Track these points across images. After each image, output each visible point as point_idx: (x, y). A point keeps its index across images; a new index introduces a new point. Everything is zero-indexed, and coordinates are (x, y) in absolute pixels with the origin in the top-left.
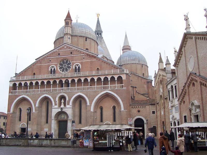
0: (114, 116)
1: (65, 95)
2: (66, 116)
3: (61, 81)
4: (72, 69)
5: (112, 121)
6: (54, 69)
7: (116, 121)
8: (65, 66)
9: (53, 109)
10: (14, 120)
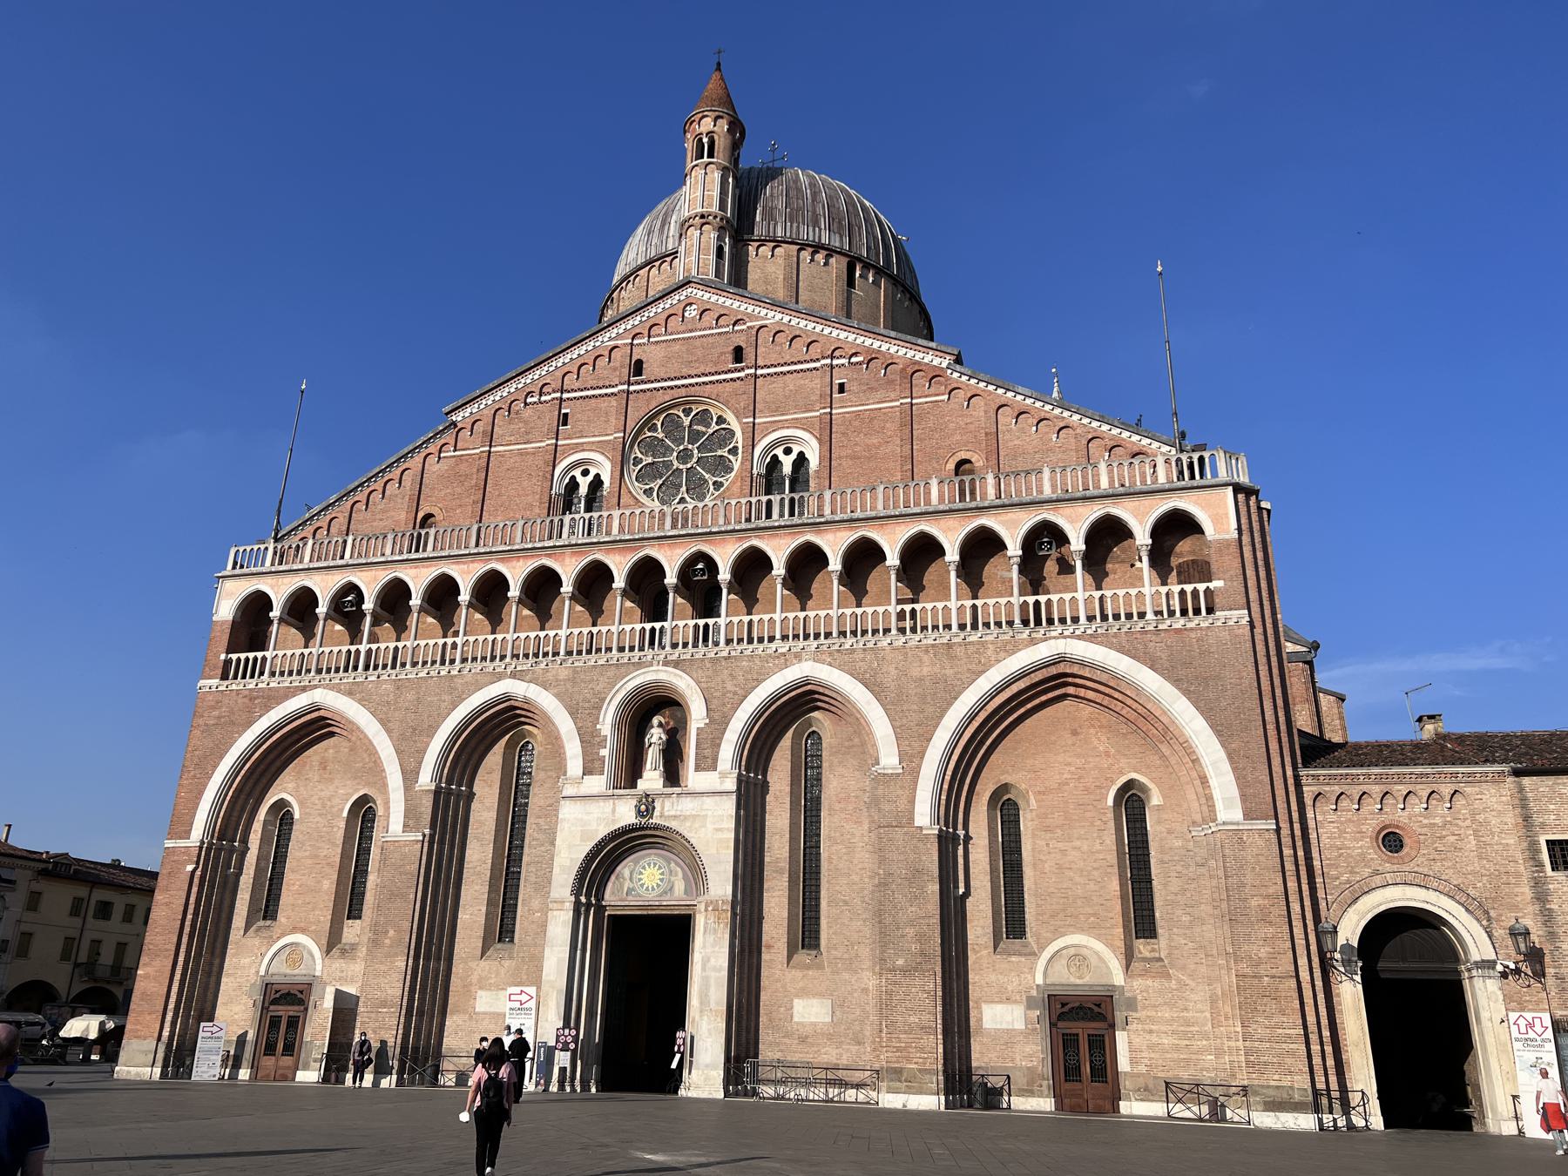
1: (684, 684)
3: (646, 575)
4: (740, 477)
7: (1160, 931)
8: (685, 456)
9: (567, 811)
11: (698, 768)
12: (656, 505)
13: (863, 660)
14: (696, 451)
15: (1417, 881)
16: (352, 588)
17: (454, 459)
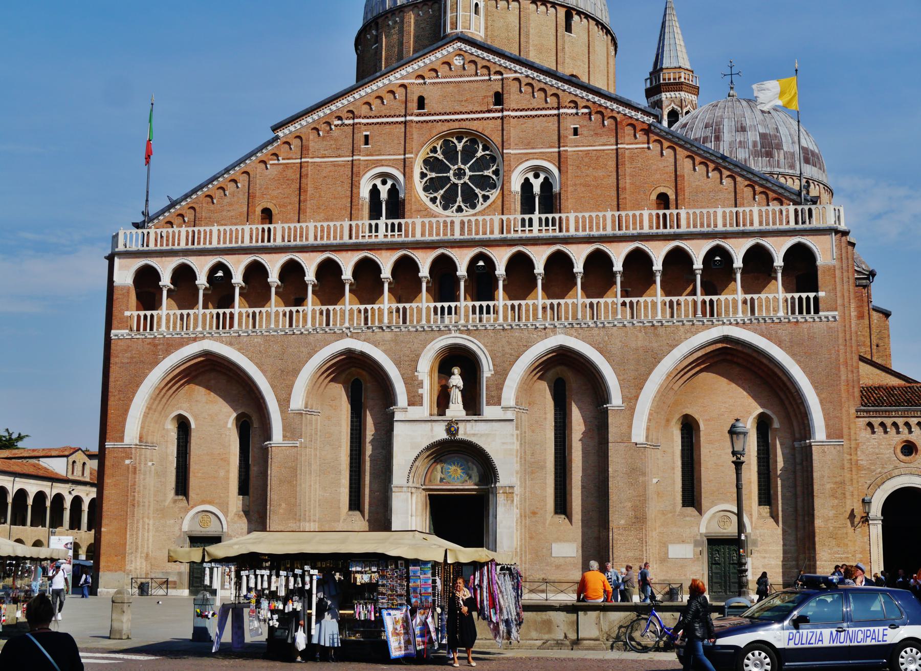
2: (475, 470)
3: (443, 267)
8: (460, 174)
9: (398, 429)
13: (599, 335)
14: (467, 171)
15: (917, 473)
17: (282, 166)
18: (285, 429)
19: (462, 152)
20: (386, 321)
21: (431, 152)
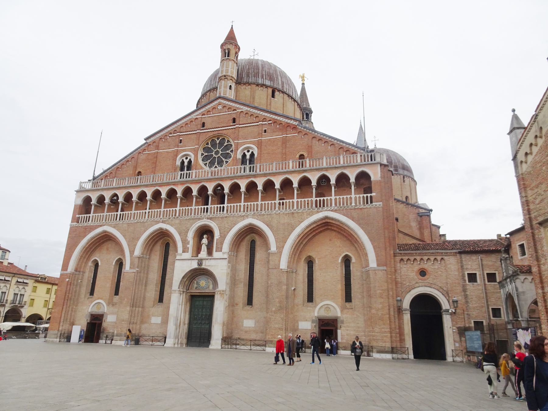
0: (346, 285)
2: (211, 283)
3: (203, 190)
4: (233, 159)
5: (342, 299)
6: (190, 162)
7: (353, 300)
8: (217, 153)
9: (177, 263)
10: (75, 292)
11: (216, 251)
12: (207, 168)
14: (220, 151)
15: (428, 285)
16: (116, 195)
18: (132, 264)
19: (219, 144)
20: (177, 215)
21: (207, 144)
